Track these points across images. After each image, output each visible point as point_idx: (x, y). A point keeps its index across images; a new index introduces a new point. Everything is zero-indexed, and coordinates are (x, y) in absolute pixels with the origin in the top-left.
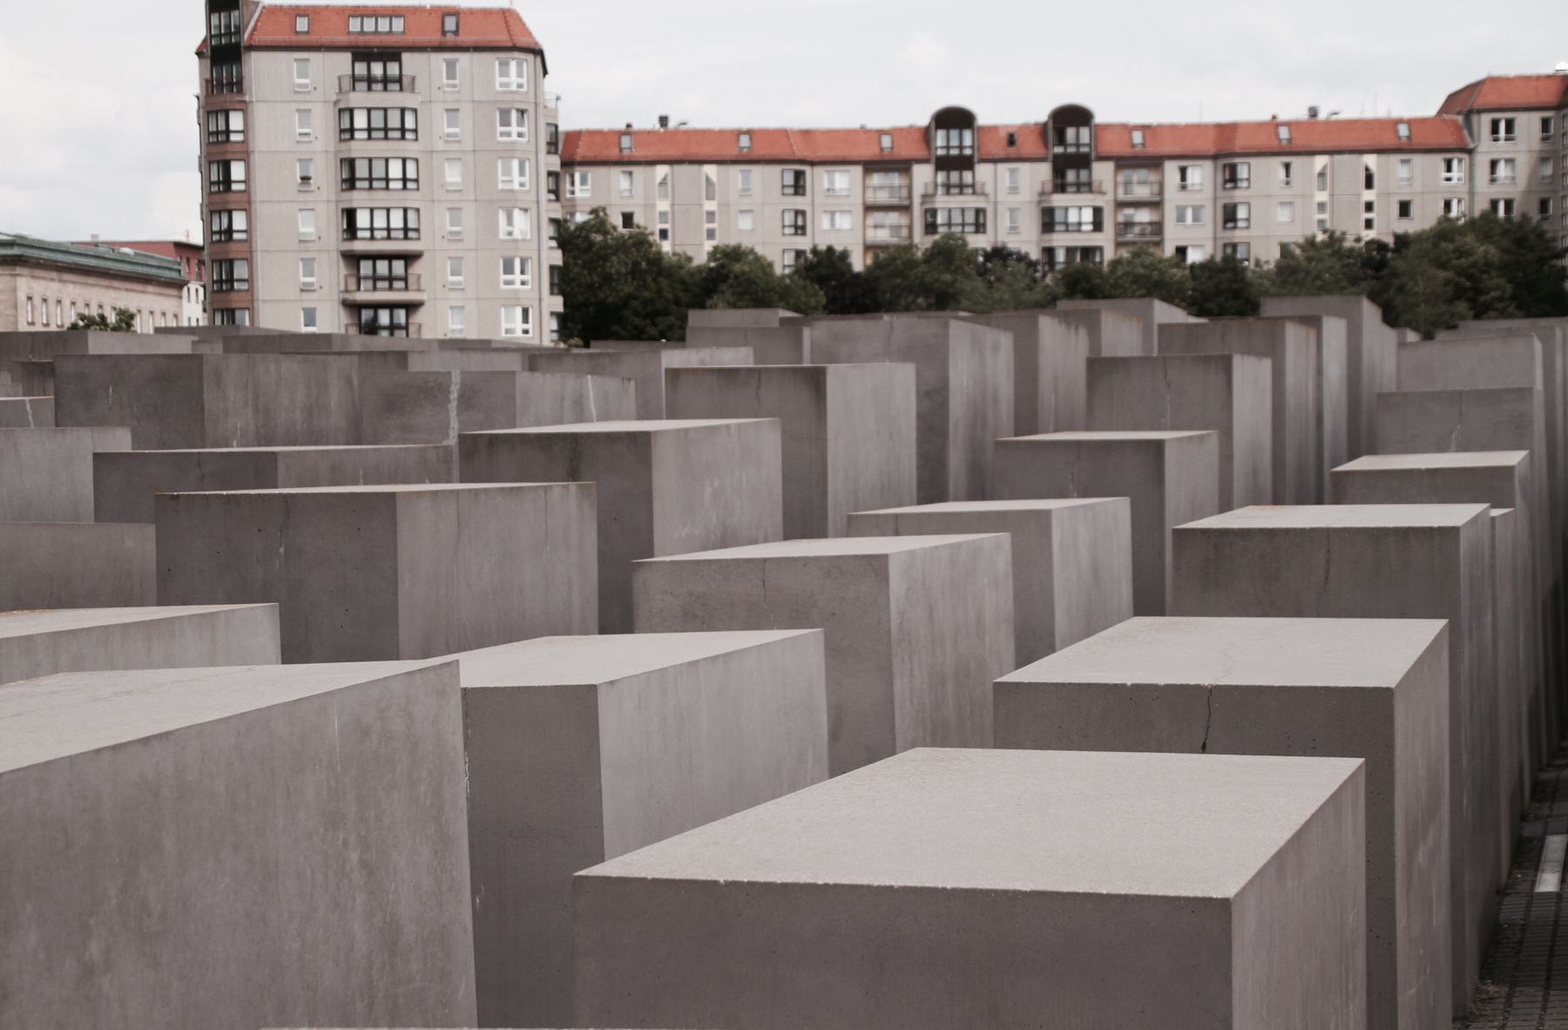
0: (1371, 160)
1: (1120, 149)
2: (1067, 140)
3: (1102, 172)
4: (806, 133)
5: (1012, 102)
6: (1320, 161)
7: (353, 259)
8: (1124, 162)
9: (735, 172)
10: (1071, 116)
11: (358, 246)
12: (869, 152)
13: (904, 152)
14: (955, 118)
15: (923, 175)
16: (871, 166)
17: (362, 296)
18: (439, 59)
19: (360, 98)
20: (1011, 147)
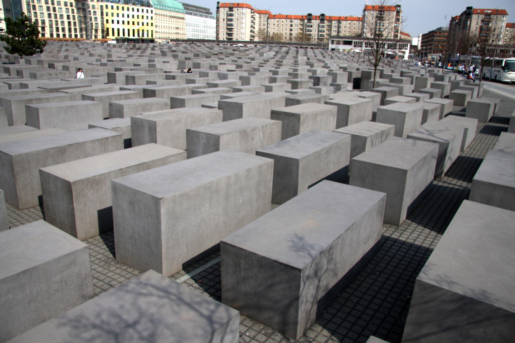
0: (355, 22)
1: (328, 18)
2: (322, 18)
3: (326, 21)
4: (294, 16)
5: (316, 13)
6: (349, 22)
7: (227, 29)
8: (328, 20)
9: (285, 20)
10: (323, 15)
11: (228, 27)
12: (301, 18)
13: (304, 18)
14: (310, 15)
15: (306, 21)
16: (300, 20)
17: (228, 32)
18: (236, 9)
19: (229, 13)
20: (316, 18)
